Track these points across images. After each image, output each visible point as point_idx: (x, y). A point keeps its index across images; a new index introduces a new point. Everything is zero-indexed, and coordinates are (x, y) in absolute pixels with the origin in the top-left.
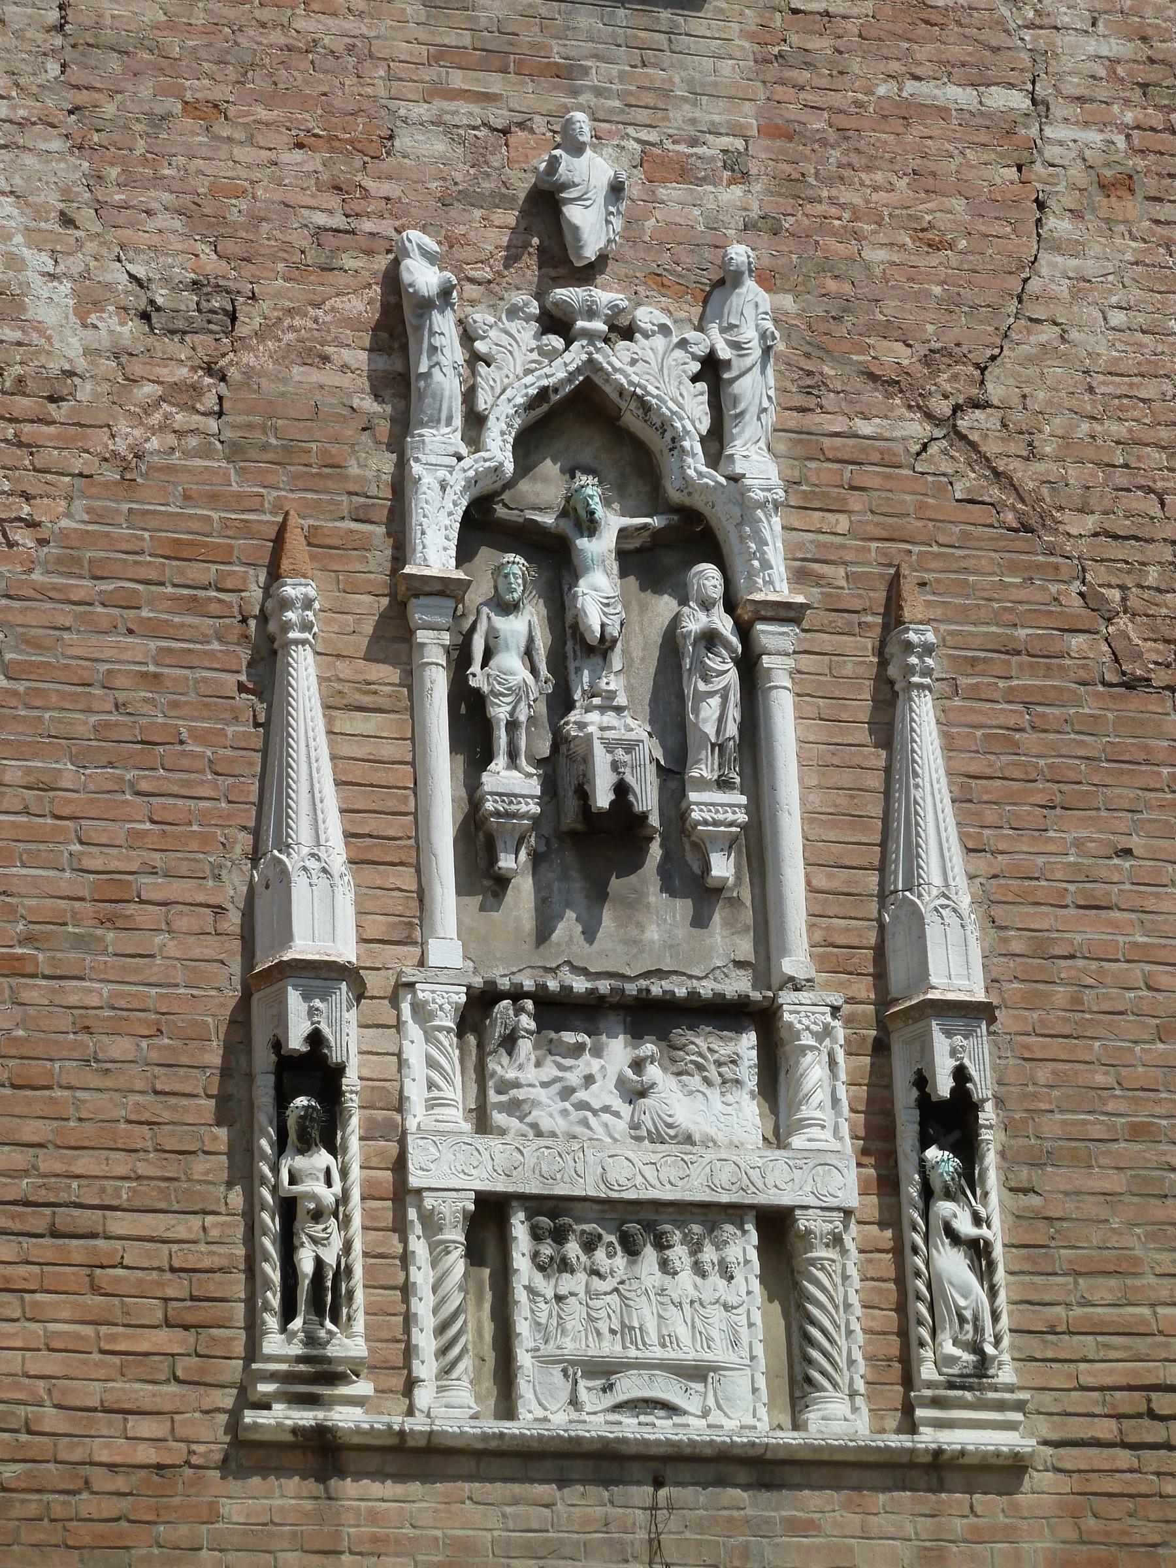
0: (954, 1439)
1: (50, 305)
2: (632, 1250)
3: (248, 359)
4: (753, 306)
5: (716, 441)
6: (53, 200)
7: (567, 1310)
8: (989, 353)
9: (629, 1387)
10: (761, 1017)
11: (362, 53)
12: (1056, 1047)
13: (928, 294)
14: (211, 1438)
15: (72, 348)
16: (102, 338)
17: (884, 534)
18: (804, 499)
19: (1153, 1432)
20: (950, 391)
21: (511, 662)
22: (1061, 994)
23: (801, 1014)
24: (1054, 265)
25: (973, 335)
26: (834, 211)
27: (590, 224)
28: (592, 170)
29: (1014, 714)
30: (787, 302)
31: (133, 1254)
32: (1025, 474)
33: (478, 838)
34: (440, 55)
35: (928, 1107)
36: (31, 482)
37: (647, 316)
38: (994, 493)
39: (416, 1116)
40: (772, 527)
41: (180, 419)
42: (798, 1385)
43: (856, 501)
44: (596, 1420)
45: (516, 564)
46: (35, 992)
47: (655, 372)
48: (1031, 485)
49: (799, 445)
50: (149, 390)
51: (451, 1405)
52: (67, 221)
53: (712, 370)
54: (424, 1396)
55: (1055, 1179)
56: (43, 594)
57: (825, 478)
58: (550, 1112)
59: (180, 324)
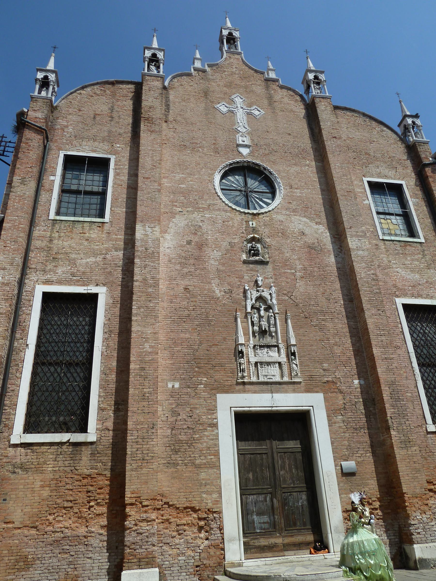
0: (295, 380)
1: (217, 292)
2: (268, 366)
4: (273, 289)
5: (271, 300)
7: (263, 371)
9: (268, 377)
10: (278, 346)
11: (241, 270)
12: (302, 348)
14: (235, 382)
15: (219, 295)
16: (221, 294)
18: (278, 304)
19: (312, 379)
20: (290, 294)
21: (256, 319)
22: (302, 343)
23: (281, 346)
25: (291, 290)
27: (260, 283)
28: (260, 279)
29: (297, 321)
31: (228, 368)
33: (254, 333)
34: (247, 270)
35: (291, 353)
36: (217, 306)
37: (265, 290)
39: (250, 356)
40: (276, 306)
42: (282, 376)
43: (283, 304)
44: (266, 380)
45: (255, 310)
46: (219, 347)
47: (266, 294)
49: (278, 300)
51: (254, 379)
53: (270, 294)
54: (252, 378)
55: (302, 358)
56: (218, 315)
58: (261, 355)
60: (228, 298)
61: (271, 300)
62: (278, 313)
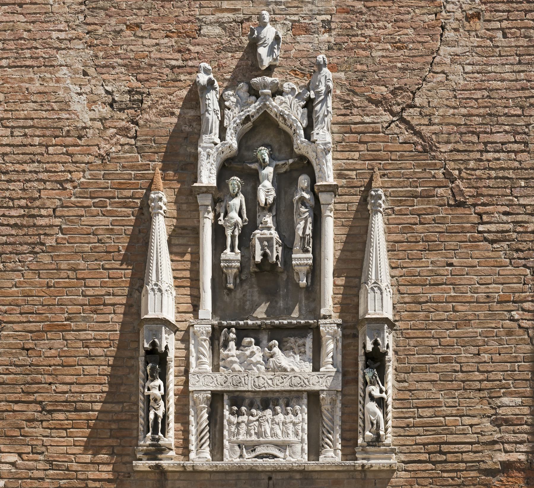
1: (79, 105)
3: (146, 116)
5: (308, 131)
6: (80, 67)
8: (417, 87)
13: (396, 67)
15: (86, 117)
17: (372, 158)
20: (399, 103)
21: (234, 215)
24: (444, 51)
25: (410, 80)
26: (363, 39)
30: (342, 75)
32: (426, 131)
36: (72, 167)
38: (415, 138)
41: (123, 140)
43: (362, 147)
47: (289, 108)
48: (429, 135)
50: (113, 131)
52: (85, 74)
57: (351, 139)
59: (123, 106)
60: (123, 131)
61: (308, 131)
62: (332, 189)
